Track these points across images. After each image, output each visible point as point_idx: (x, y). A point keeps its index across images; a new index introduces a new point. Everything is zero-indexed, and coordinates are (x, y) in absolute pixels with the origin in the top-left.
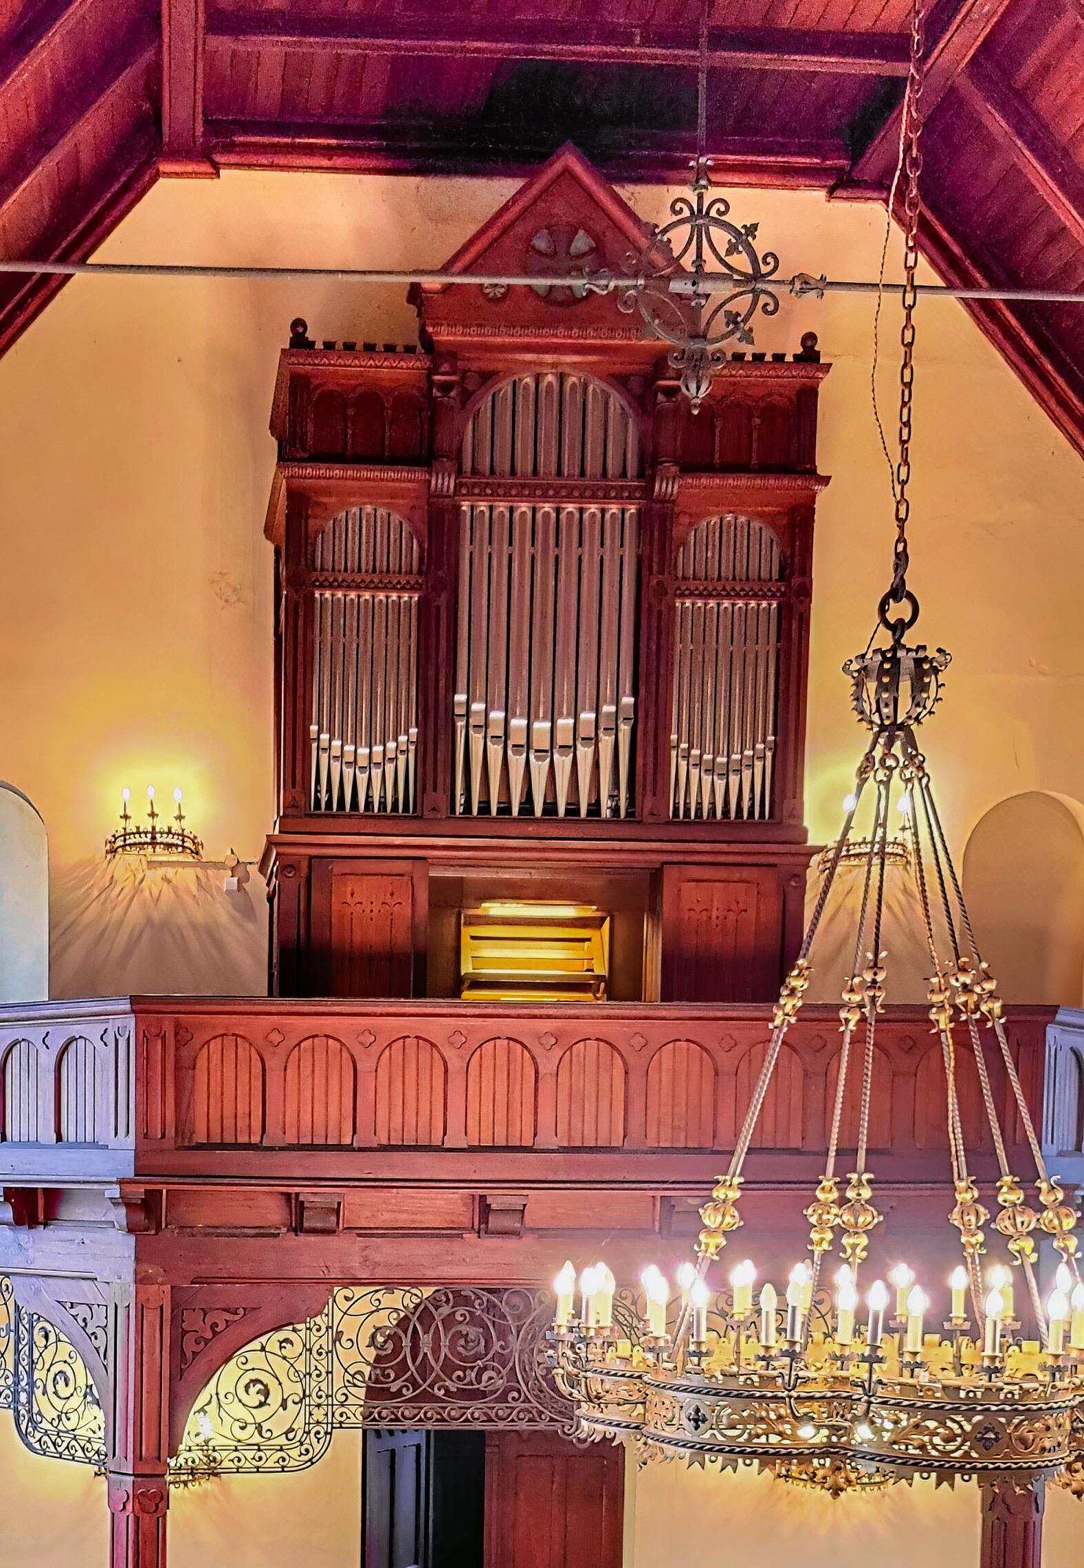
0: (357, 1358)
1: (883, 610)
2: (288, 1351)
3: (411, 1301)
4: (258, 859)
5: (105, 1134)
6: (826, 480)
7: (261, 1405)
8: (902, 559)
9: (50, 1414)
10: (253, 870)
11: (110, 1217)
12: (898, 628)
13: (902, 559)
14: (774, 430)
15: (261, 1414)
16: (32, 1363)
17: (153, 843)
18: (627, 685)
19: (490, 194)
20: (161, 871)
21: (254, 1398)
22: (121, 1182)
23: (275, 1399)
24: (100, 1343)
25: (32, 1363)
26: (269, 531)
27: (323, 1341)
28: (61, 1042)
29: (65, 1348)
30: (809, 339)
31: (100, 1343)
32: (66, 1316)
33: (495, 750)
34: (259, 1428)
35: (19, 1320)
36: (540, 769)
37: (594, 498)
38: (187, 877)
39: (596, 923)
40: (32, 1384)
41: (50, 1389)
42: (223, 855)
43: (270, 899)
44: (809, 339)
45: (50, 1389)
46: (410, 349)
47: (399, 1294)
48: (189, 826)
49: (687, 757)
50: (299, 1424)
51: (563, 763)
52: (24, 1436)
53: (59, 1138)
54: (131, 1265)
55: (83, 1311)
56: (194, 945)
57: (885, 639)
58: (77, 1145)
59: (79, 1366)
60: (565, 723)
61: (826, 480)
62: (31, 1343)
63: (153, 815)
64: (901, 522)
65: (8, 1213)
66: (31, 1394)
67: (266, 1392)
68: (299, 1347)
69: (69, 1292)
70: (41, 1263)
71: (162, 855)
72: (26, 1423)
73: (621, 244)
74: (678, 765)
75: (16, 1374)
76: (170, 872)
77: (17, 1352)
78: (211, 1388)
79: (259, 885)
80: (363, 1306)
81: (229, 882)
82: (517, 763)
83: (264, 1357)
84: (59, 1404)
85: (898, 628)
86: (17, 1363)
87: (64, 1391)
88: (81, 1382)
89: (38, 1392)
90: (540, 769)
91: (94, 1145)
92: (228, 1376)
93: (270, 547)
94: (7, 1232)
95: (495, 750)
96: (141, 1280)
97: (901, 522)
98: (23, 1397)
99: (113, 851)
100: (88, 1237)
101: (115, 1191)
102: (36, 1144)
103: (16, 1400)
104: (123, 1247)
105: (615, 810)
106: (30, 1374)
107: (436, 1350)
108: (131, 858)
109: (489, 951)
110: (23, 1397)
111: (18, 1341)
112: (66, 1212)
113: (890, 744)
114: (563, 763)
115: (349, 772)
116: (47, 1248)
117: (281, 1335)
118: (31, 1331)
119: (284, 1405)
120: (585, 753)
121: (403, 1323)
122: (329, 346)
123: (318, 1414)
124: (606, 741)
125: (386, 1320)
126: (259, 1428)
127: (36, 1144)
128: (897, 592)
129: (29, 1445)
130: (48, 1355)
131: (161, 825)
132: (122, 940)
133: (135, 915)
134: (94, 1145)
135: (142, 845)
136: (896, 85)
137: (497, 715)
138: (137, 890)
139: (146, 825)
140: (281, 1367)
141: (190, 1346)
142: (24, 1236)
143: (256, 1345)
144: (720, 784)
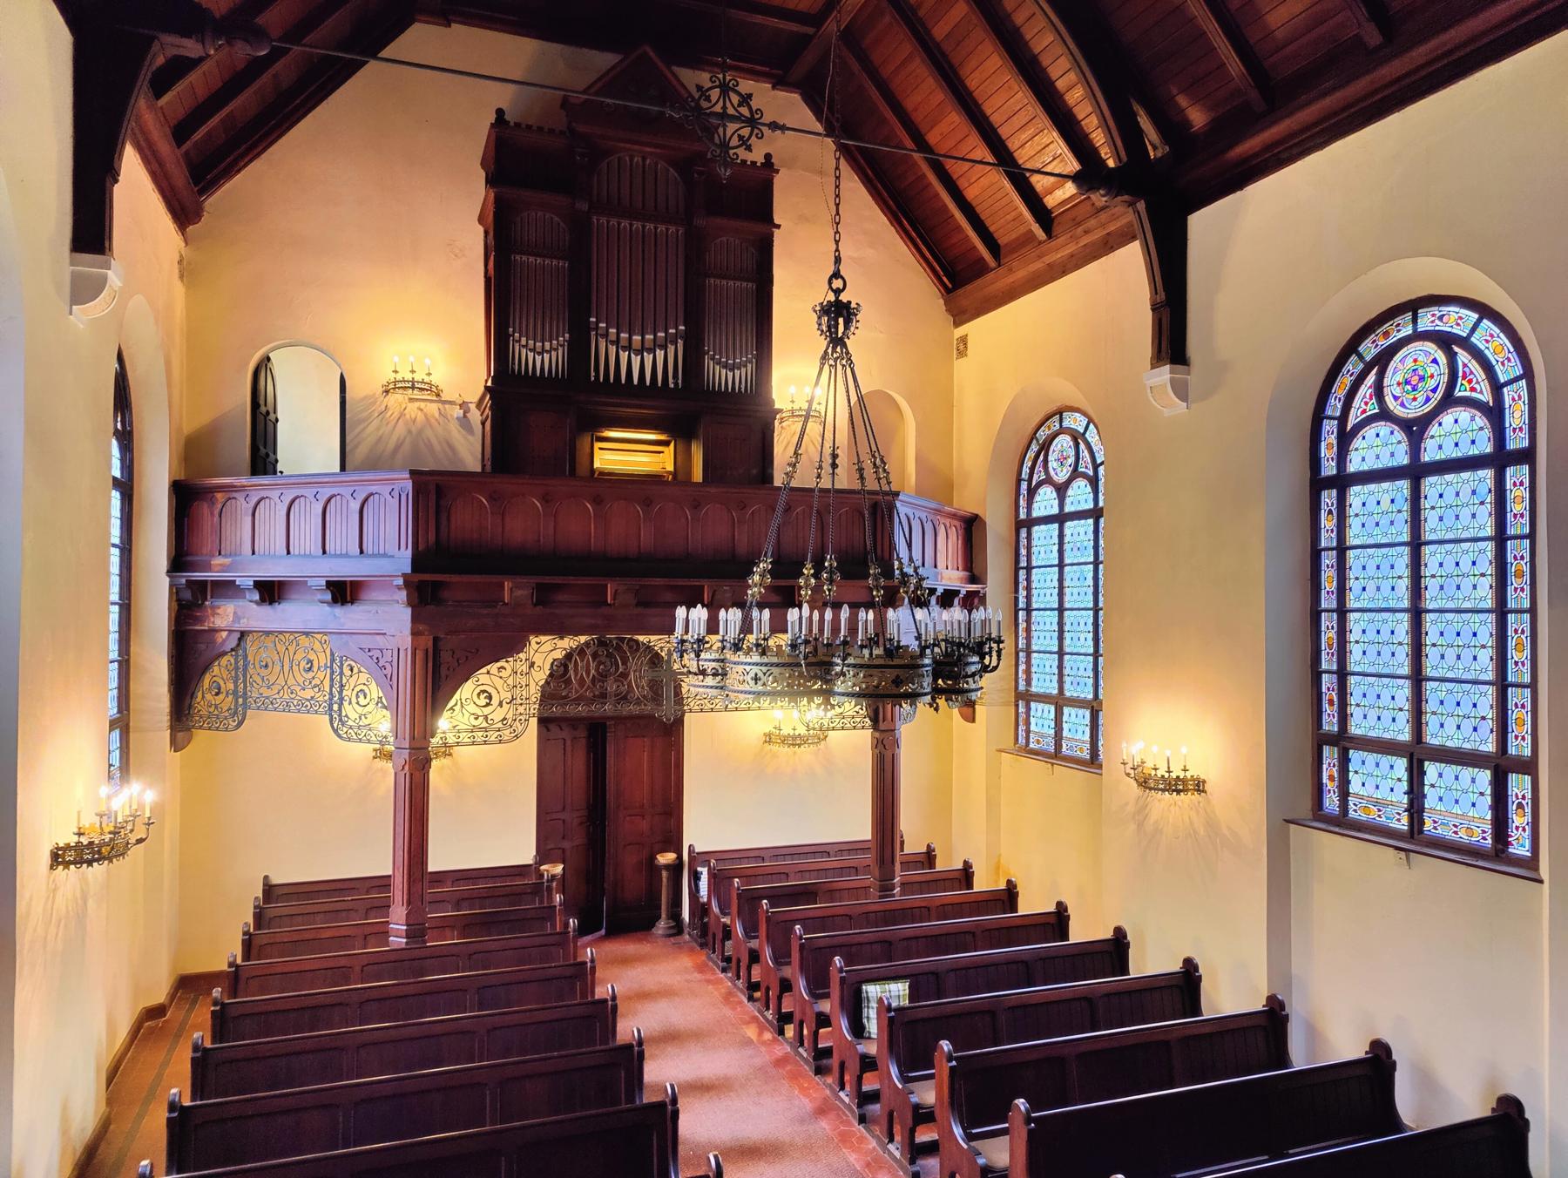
0: (540, 676)
1: (830, 282)
2: (504, 674)
3: (574, 644)
4: (476, 399)
5: (391, 548)
6: (778, 227)
7: (488, 705)
8: (838, 260)
9: (353, 715)
10: (473, 407)
11: (396, 597)
12: (837, 292)
13: (838, 260)
14: (751, 200)
15: (487, 711)
16: (342, 686)
17: (413, 388)
18: (681, 319)
19: (604, 60)
20: (417, 404)
21: (483, 701)
22: (404, 575)
23: (495, 701)
24: (388, 671)
25: (342, 686)
26: (481, 220)
27: (525, 668)
28: (363, 496)
29: (364, 677)
30: (768, 156)
31: (388, 671)
32: (365, 656)
33: (612, 349)
34: (486, 717)
35: (333, 660)
36: (636, 361)
37: (663, 222)
38: (433, 409)
39: (666, 443)
40: (341, 699)
41: (354, 700)
42: (454, 397)
43: (483, 424)
44: (768, 156)
45: (354, 700)
46: (561, 132)
47: (566, 640)
48: (435, 379)
49: (713, 359)
50: (510, 716)
51: (648, 358)
52: (336, 731)
53: (362, 552)
54: (409, 625)
55: (377, 654)
56: (437, 447)
57: (831, 297)
58: (373, 556)
59: (373, 686)
60: (649, 337)
61: (778, 227)
62: (341, 674)
63: (413, 372)
64: (837, 242)
65: (329, 597)
66: (340, 705)
67: (490, 697)
68: (509, 671)
69: (366, 642)
70: (349, 626)
71: (416, 394)
72: (338, 722)
73: (671, 93)
74: (708, 363)
75: (331, 693)
76: (422, 405)
77: (332, 680)
78: (457, 696)
79: (475, 416)
80: (547, 647)
81: (458, 412)
82: (624, 356)
83: (493, 678)
84: (360, 709)
85: (837, 292)
86: (332, 686)
87: (362, 701)
88: (375, 696)
89: (346, 704)
90: (636, 361)
91: (385, 555)
92: (467, 690)
93: (481, 229)
94: (326, 608)
95: (612, 349)
96: (415, 633)
97: (837, 242)
98: (336, 707)
99: (387, 392)
100: (381, 609)
101: (400, 581)
102: (347, 556)
103: (331, 708)
104: (406, 614)
105: (676, 384)
106: (341, 693)
107: (588, 673)
108: (396, 399)
109: (609, 456)
110: (336, 707)
111: (332, 673)
112: (364, 595)
113: (834, 350)
114: (648, 358)
115: (531, 355)
116: (352, 617)
117: (499, 664)
118: (341, 667)
119: (501, 704)
120: (660, 354)
121: (569, 656)
122: (517, 125)
123: (521, 709)
124: (671, 349)
125: (559, 654)
126: (486, 717)
127: (347, 556)
128: (836, 275)
129: (339, 736)
130: (352, 681)
131: (418, 377)
132: (391, 445)
133: (401, 430)
134: (385, 555)
135: (405, 388)
136: (807, 39)
137: (613, 331)
138: (402, 415)
139: (409, 377)
140: (499, 683)
141: (443, 672)
142: (339, 610)
143: (484, 670)
144: (730, 375)
